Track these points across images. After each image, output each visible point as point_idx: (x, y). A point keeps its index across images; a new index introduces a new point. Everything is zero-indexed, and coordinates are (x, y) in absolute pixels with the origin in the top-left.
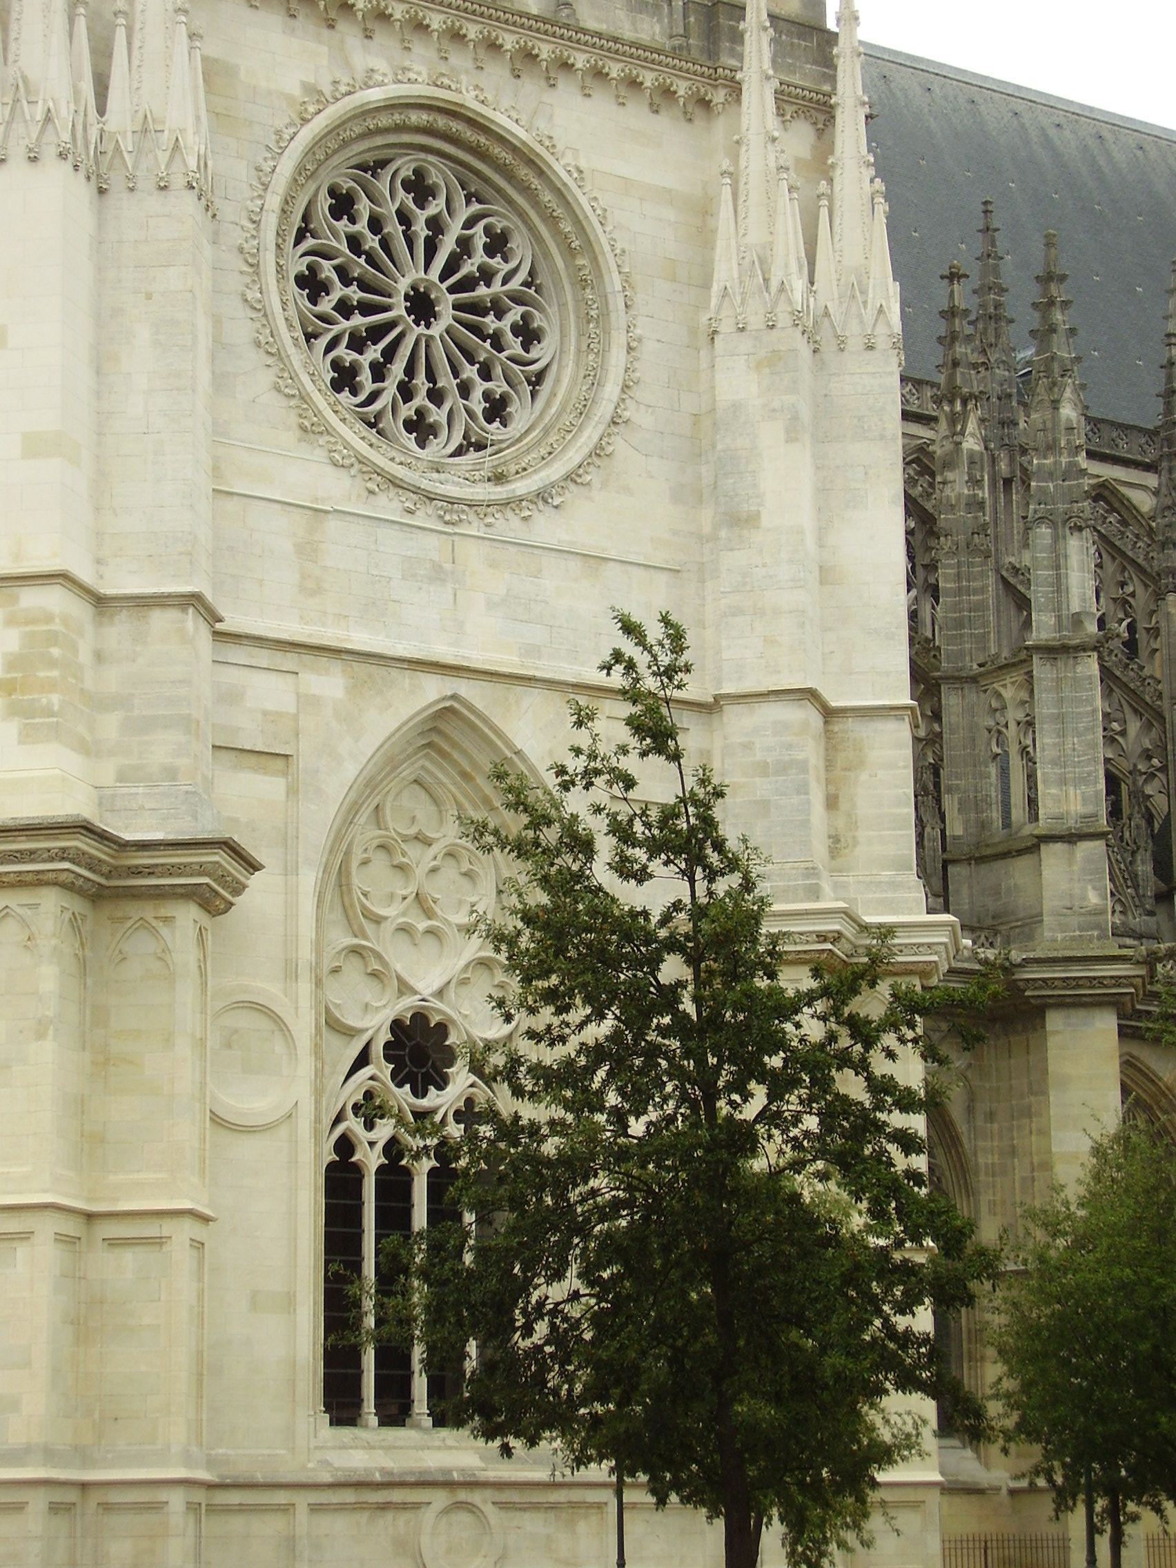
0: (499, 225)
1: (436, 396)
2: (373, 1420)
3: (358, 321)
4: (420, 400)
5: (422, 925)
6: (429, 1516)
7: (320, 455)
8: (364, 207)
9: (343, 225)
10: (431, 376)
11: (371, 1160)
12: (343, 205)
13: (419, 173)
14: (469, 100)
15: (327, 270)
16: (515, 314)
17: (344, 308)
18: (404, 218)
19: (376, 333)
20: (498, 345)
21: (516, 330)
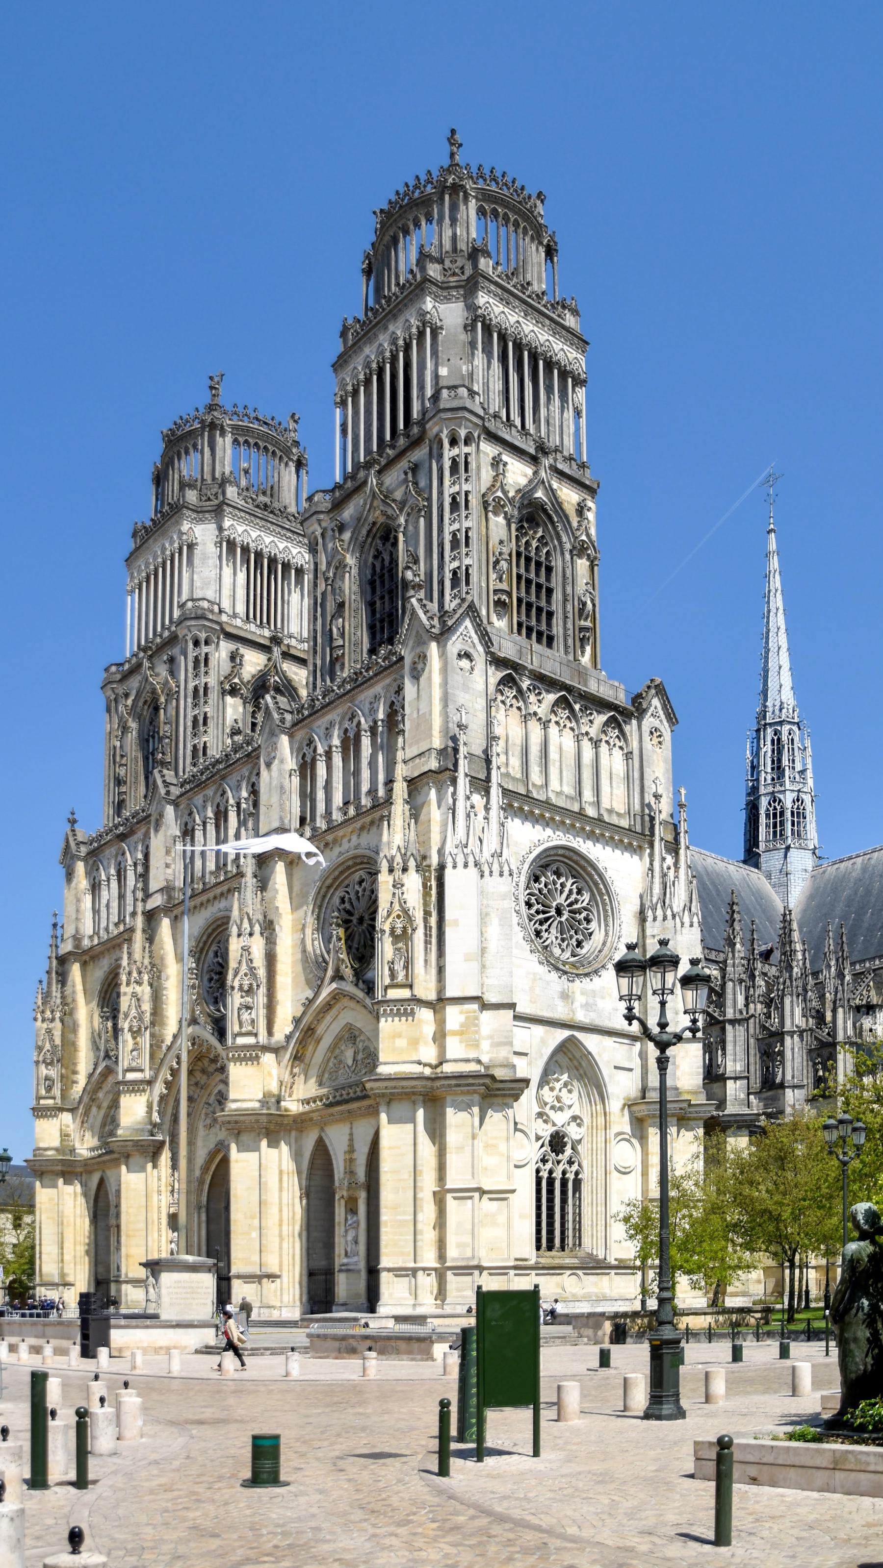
3: (541, 916)
6: (565, 1276)
8: (543, 879)
15: (533, 900)
16: (584, 914)
18: (555, 883)
21: (585, 919)
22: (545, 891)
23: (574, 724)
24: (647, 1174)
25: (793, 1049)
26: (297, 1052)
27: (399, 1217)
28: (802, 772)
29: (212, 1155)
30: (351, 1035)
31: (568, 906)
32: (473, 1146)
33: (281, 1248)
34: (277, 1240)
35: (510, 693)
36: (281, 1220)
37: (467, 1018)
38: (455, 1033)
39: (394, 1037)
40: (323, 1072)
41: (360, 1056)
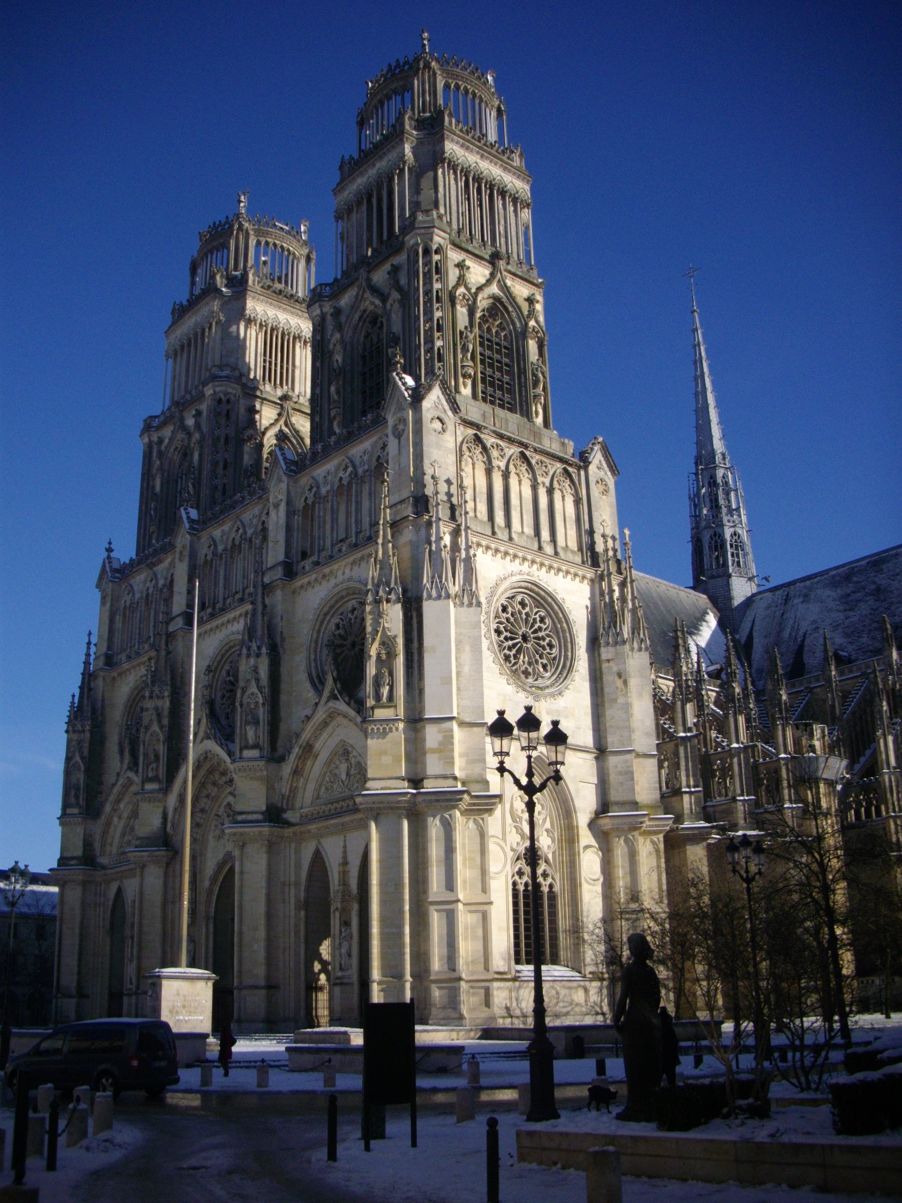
3: (510, 643)
7: (505, 681)
8: (510, 609)
9: (505, 615)
11: (521, 888)
12: (504, 609)
13: (522, 600)
16: (548, 639)
17: (506, 639)
18: (520, 613)
19: (514, 645)
22: (512, 619)
26: (297, 766)
29: (221, 866)
31: (533, 633)
37: (444, 737)
38: (434, 751)
40: (320, 786)
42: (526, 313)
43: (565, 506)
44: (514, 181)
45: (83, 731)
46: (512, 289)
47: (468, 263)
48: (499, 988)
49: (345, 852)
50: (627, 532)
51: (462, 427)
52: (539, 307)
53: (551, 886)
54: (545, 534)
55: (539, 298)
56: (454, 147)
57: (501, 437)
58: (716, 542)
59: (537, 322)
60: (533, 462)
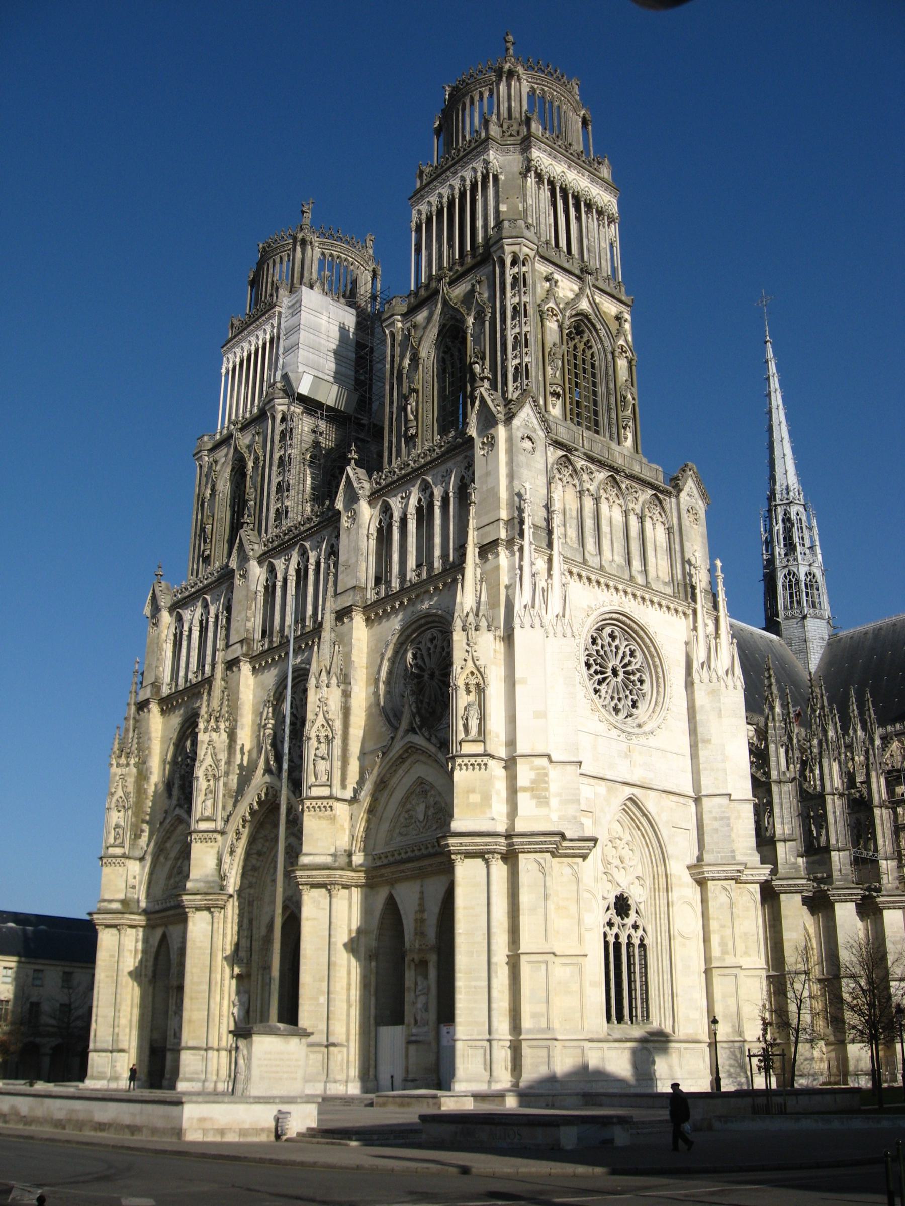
0: (633, 647)
1: (619, 700)
2: (616, 1022)
3: (600, 677)
4: (616, 701)
5: (622, 866)
8: (599, 641)
9: (594, 647)
10: (618, 694)
11: (612, 939)
12: (594, 642)
13: (613, 632)
14: (627, 610)
15: (592, 661)
16: (638, 675)
17: (596, 672)
18: (610, 645)
19: (604, 679)
20: (635, 685)
23: (622, 501)
24: (710, 941)
25: (834, 812)
27: (473, 984)
28: (812, 548)
30: (422, 788)
31: (623, 667)
32: (545, 908)
33: (348, 1015)
34: (345, 1006)
35: (567, 472)
36: (349, 985)
37: (538, 774)
38: (525, 790)
39: (468, 792)
41: (431, 812)
42: (614, 332)
43: (657, 534)
44: (601, 193)
45: (128, 765)
46: (601, 306)
47: (556, 276)
48: (591, 1048)
49: (422, 899)
50: (719, 563)
51: (551, 448)
52: (627, 326)
53: (642, 940)
54: (637, 564)
55: (627, 316)
56: (541, 155)
57: (591, 459)
58: (790, 581)
59: (627, 341)
60: (623, 486)
